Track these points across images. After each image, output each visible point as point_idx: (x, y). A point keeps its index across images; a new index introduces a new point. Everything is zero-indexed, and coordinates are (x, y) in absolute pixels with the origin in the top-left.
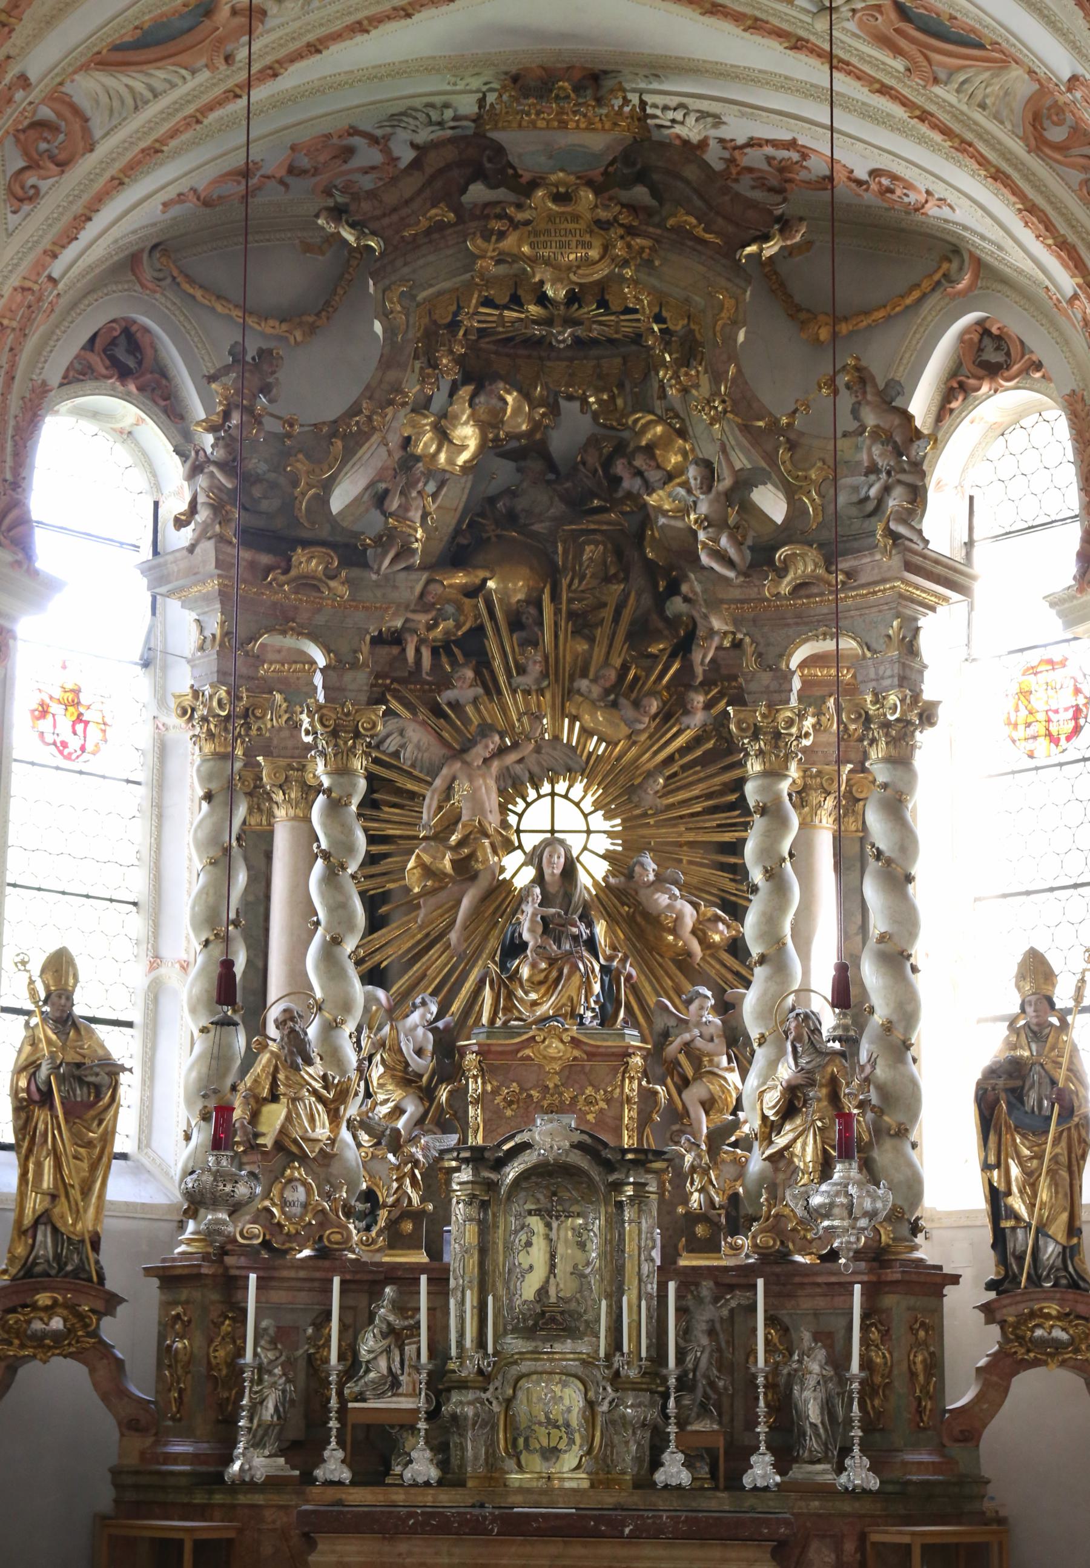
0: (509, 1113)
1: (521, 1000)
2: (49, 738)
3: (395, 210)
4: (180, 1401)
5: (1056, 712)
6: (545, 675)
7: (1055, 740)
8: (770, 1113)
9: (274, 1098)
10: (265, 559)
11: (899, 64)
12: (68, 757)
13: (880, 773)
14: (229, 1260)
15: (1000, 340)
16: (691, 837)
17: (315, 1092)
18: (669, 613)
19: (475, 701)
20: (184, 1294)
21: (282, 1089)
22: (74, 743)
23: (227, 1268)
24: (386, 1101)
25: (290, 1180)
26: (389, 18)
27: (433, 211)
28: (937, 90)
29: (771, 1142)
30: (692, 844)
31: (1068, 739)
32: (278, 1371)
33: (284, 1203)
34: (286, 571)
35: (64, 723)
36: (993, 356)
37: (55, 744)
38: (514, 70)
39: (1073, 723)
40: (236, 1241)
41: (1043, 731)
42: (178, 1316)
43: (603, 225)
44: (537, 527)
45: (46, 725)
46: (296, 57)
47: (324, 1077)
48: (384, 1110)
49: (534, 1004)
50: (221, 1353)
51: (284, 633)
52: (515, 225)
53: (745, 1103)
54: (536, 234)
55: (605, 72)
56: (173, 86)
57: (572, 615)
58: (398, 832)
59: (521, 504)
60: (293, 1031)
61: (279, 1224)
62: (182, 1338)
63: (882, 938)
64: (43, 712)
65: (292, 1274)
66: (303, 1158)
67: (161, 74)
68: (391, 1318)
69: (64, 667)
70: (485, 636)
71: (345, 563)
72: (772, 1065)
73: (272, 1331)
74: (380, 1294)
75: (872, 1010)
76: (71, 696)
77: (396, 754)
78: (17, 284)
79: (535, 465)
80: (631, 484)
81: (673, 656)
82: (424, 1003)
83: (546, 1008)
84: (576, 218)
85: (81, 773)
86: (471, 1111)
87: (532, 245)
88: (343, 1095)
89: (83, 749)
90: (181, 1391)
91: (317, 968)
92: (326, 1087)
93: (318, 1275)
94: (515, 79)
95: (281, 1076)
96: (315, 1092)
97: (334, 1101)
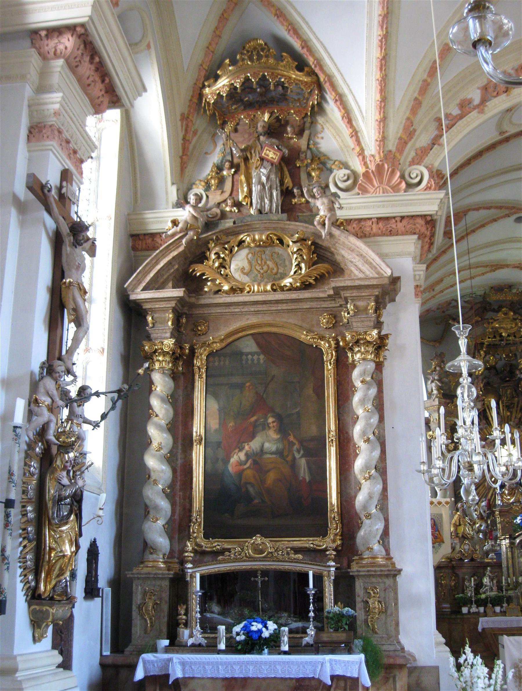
0: (507, 525)
1: (505, 498)
3: (467, 318)
4: (444, 595)
9: (460, 525)
10: (448, 401)
14: (454, 563)
17: (469, 523)
19: (486, 428)
20: (443, 571)
21: (461, 523)
23: (453, 564)
25: (465, 544)
33: (464, 550)
34: (452, 403)
38: (492, 286)
42: (442, 576)
43: (515, 319)
44: (495, 386)
46: (447, 288)
49: (509, 499)
50: (453, 584)
51: (451, 417)
52: (495, 320)
54: (500, 322)
55: (513, 285)
57: (506, 406)
59: (490, 380)
61: (464, 554)
62: (444, 580)
66: (467, 538)
68: (490, 574)
74: (487, 569)
79: (493, 371)
83: (511, 501)
84: (509, 318)
86: (498, 525)
87: (499, 325)
90: (444, 593)
91: (464, 494)
94: (492, 288)
95: (461, 520)
96: (469, 523)
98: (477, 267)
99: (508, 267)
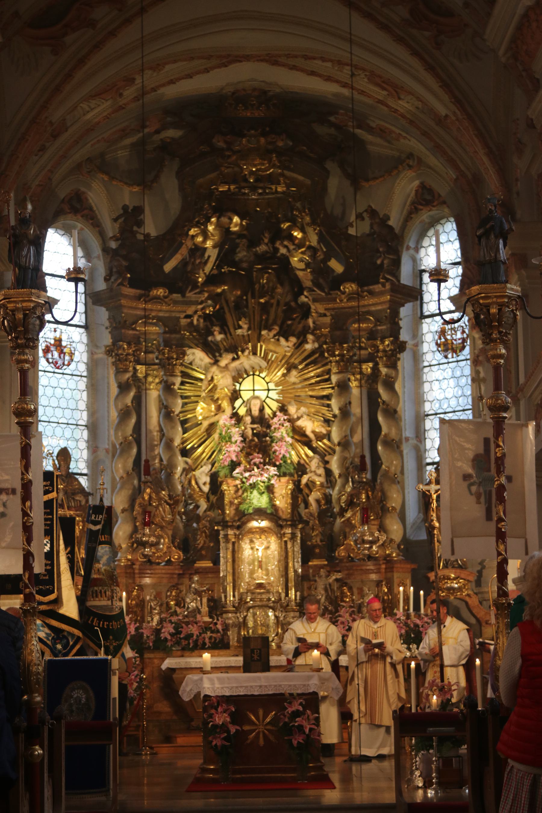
2: (51, 361)
5: (455, 340)
6: (249, 329)
7: (454, 351)
8: (343, 505)
11: (385, 93)
12: (58, 368)
13: (384, 371)
15: (430, 191)
16: (311, 393)
17: (166, 502)
18: (299, 302)
22: (60, 362)
24: (191, 504)
26: (183, 78)
27: (201, 147)
28: (400, 102)
29: (343, 516)
30: (311, 396)
31: (460, 351)
32: (158, 608)
35: (56, 354)
36: (428, 197)
37: (52, 363)
39: (461, 345)
40: (137, 559)
41: (450, 347)
45: (50, 356)
47: (169, 495)
48: (191, 507)
53: (334, 501)
56: (99, 105)
58: (191, 394)
60: (156, 477)
63: (386, 435)
64: (47, 350)
65: (160, 571)
67: (94, 102)
69: (55, 331)
70: (224, 312)
71: (171, 292)
72: (344, 486)
73: (154, 593)
75: (382, 464)
76: (58, 343)
77: (191, 364)
78: (37, 183)
80: (283, 251)
81: (302, 319)
82: (205, 465)
85: (63, 374)
88: (177, 502)
89: (64, 364)
92: (170, 499)
93: (169, 572)
96: (166, 502)
97: (173, 504)
98: (192, 59)
99: (248, 60)
